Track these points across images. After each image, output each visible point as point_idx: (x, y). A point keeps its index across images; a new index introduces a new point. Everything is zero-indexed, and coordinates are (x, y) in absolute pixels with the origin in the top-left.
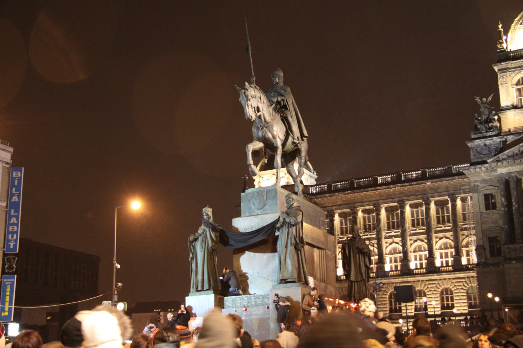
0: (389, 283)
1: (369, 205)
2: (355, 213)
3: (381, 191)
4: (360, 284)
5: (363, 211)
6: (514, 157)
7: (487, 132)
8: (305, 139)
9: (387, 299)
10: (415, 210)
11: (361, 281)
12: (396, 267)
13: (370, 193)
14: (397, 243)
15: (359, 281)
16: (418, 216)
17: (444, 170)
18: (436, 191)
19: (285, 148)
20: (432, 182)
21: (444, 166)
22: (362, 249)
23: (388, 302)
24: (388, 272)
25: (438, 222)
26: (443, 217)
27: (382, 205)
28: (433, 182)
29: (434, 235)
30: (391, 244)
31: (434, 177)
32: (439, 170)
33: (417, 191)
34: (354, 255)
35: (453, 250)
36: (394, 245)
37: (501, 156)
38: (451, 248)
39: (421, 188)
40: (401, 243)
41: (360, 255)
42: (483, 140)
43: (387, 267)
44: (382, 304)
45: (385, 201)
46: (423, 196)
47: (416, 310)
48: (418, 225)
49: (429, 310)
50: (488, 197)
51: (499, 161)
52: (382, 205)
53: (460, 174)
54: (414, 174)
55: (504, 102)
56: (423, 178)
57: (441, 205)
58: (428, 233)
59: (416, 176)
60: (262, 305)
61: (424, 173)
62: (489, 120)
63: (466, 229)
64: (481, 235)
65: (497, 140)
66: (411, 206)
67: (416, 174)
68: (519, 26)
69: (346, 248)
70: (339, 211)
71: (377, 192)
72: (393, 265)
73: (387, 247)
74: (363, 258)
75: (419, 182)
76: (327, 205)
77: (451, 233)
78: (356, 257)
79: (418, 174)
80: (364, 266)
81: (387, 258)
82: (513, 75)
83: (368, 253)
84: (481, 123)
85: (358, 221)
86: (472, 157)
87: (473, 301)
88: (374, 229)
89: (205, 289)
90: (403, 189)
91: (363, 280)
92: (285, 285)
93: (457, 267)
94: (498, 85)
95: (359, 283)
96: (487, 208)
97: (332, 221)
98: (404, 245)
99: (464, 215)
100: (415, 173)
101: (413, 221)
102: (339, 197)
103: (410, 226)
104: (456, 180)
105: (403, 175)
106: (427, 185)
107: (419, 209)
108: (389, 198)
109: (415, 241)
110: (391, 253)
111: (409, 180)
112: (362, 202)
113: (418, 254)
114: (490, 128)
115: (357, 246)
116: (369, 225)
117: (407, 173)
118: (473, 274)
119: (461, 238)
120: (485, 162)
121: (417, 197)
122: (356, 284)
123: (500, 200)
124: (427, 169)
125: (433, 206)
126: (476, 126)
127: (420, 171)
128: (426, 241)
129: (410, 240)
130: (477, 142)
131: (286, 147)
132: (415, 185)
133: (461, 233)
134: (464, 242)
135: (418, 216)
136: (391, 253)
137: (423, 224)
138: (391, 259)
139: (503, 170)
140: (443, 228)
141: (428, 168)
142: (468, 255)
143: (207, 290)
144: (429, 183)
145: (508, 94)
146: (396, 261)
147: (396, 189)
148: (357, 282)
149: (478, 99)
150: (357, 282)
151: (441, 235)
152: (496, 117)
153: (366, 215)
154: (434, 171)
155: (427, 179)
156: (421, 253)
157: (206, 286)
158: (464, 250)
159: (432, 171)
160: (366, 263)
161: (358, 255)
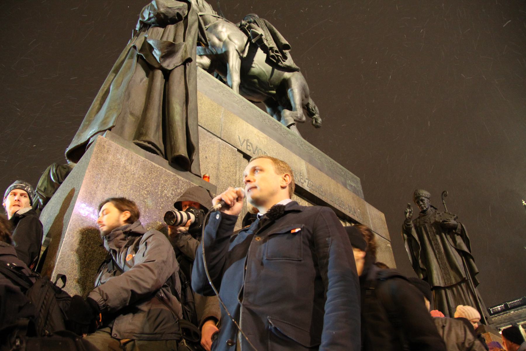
4: (458, 290)
8: (287, 52)
11: (459, 284)
15: (455, 286)
17: (520, 301)
19: (254, 67)
20: (514, 311)
21: (519, 298)
22: (444, 221)
28: (516, 310)
31: (514, 307)
32: (516, 302)
33: (505, 319)
34: (431, 238)
39: (508, 316)
41: (443, 234)
46: (511, 322)
54: (499, 308)
56: (507, 309)
59: (501, 309)
61: (506, 306)
67: (500, 307)
69: (410, 229)
74: (450, 240)
75: (505, 312)
78: (437, 240)
79: (502, 307)
80: (456, 253)
83: (459, 227)
90: (494, 319)
91: (464, 280)
95: (454, 289)
100: (499, 306)
105: (491, 310)
106: (512, 314)
115: (432, 222)
117: (494, 307)
121: (507, 323)
122: (449, 292)
124: (507, 302)
127: (503, 305)
131: (253, 65)
132: (502, 315)
141: (508, 302)
144: (512, 312)
148: (450, 287)
150: (450, 287)
154: (514, 303)
159: (512, 303)
160: (459, 245)
161: (438, 237)
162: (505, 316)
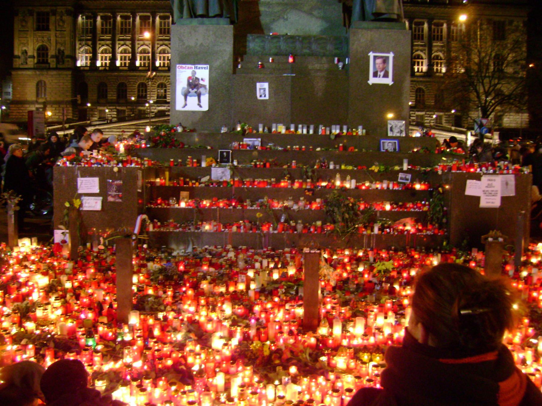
0: (138, 76)
1: (127, 12)
2: (115, 18)
5: (121, 17)
9: (136, 88)
10: (163, 21)
12: (145, 63)
14: (147, 46)
16: (165, 26)
23: (136, 90)
24: (138, 67)
27: (137, 14)
30: (142, 45)
36: (145, 47)
40: (151, 46)
43: (138, 63)
44: (132, 91)
45: (141, 10)
47: (157, 98)
48: (165, 33)
49: (168, 98)
52: (137, 14)
60: (324, 55)
66: (160, 17)
70: (101, 14)
72: (142, 62)
73: (139, 48)
81: (138, 56)
85: (117, 24)
88: (129, 32)
89: (211, 14)
92: (378, 24)
97: (95, 21)
98: (153, 48)
101: (161, 29)
103: (158, 33)
107: (167, 21)
109: (161, 45)
110: (141, 53)
113: (161, 55)
116: (126, 29)
129: (158, 44)
135: (165, 26)
136: (141, 53)
138: (141, 57)
143: (214, 17)
146: (144, 59)
153: (124, 20)
156: (164, 55)
157: (214, 9)
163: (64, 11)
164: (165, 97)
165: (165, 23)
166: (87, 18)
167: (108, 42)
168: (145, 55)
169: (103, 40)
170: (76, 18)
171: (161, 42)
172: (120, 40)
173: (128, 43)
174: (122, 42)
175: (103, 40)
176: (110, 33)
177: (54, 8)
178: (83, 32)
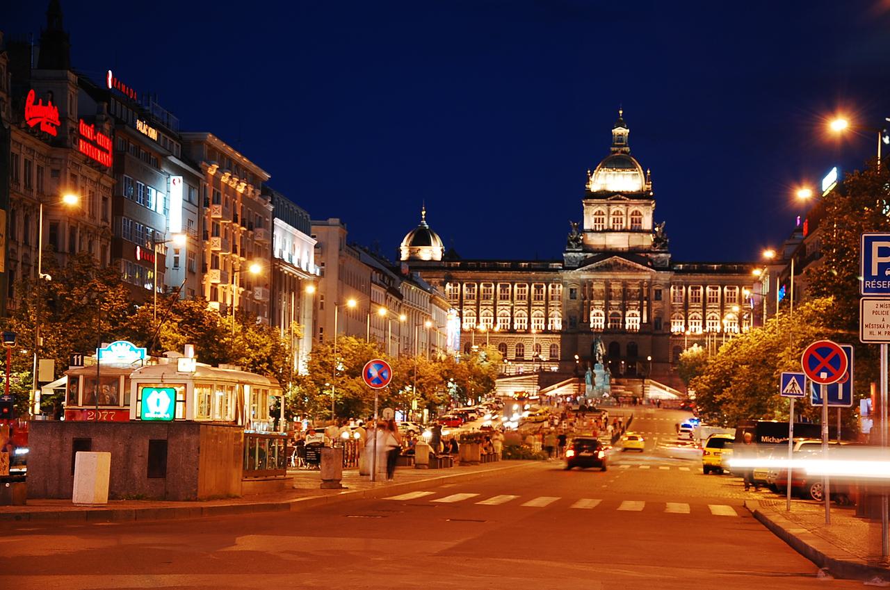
3: (501, 274)
6: (589, 269)
7: (576, 248)
10: (520, 289)
13: (494, 275)
18: (537, 279)
25: (535, 299)
26: (539, 296)
29: (532, 308)
35: (543, 319)
36: (504, 311)
37: (584, 268)
38: (542, 317)
42: (573, 254)
50: (571, 290)
51: (583, 270)
53: (556, 270)
55: (586, 227)
56: (529, 269)
57: (538, 288)
58: (529, 305)
62: (577, 240)
63: (553, 306)
64: (565, 314)
65: (582, 254)
66: (518, 286)
68: (599, 172)
71: (497, 274)
76: (459, 278)
77: (544, 308)
82: (593, 208)
84: (573, 241)
86: (565, 263)
87: (552, 353)
93: (546, 332)
94: (583, 214)
96: (571, 298)
98: (512, 313)
99: (552, 296)
102: (469, 274)
104: (552, 274)
108: (505, 279)
111: (522, 270)
112: (485, 279)
114: (578, 246)
118: (559, 336)
119: (549, 311)
120: (575, 269)
123: (579, 294)
125: (533, 288)
126: (569, 242)
128: (527, 311)
130: (569, 254)
133: (549, 308)
134: (550, 315)
137: (525, 299)
139: (585, 276)
140: (538, 304)
142: (552, 323)
145: (589, 221)
147: (510, 274)
149: (572, 224)
151: (536, 308)
152: (581, 238)
153: (485, 288)
155: (533, 270)
156: (522, 318)
158: (550, 319)
162: (525, 275)
163: (437, 282)
164: (523, 355)
165: (522, 290)
166: (454, 286)
167: (472, 307)
168: (504, 318)
169: (468, 305)
170: (445, 287)
171: (519, 308)
172: (482, 305)
173: (489, 307)
174: (485, 307)
175: (468, 305)
176: (474, 299)
177: (429, 280)
178: (450, 298)
